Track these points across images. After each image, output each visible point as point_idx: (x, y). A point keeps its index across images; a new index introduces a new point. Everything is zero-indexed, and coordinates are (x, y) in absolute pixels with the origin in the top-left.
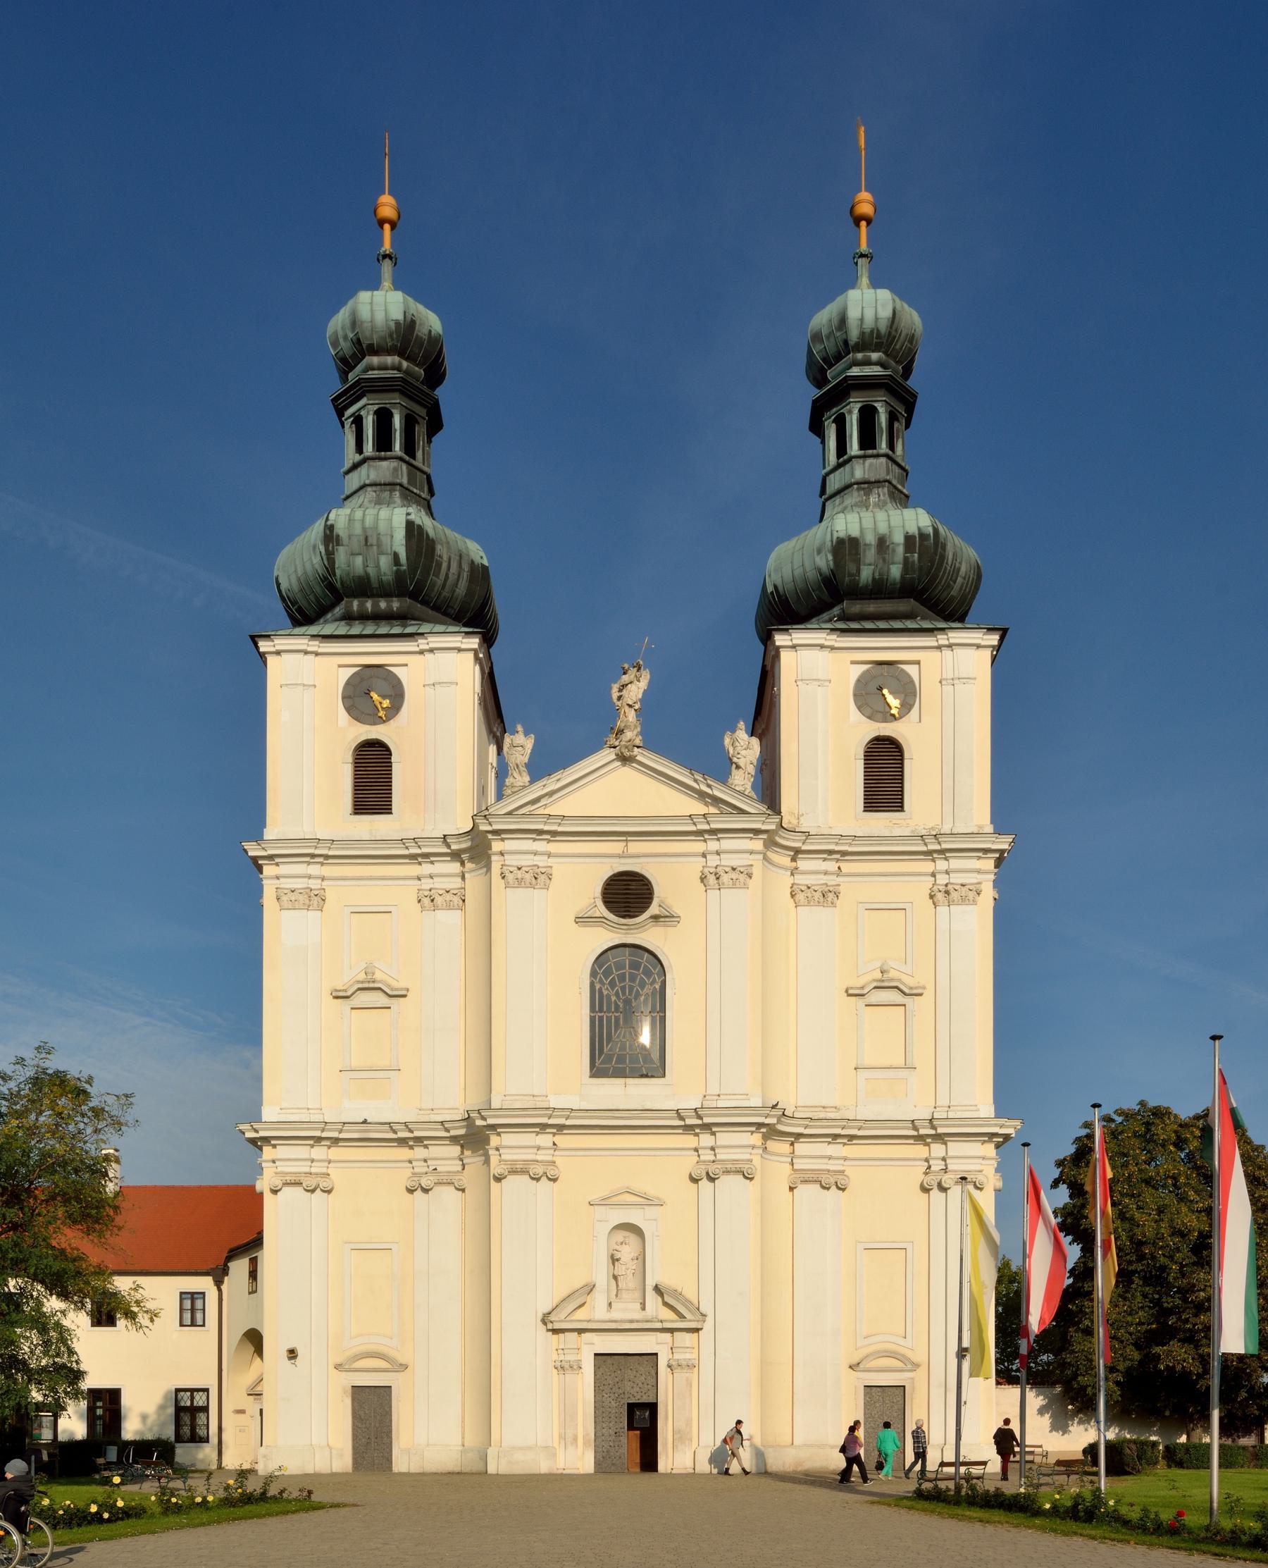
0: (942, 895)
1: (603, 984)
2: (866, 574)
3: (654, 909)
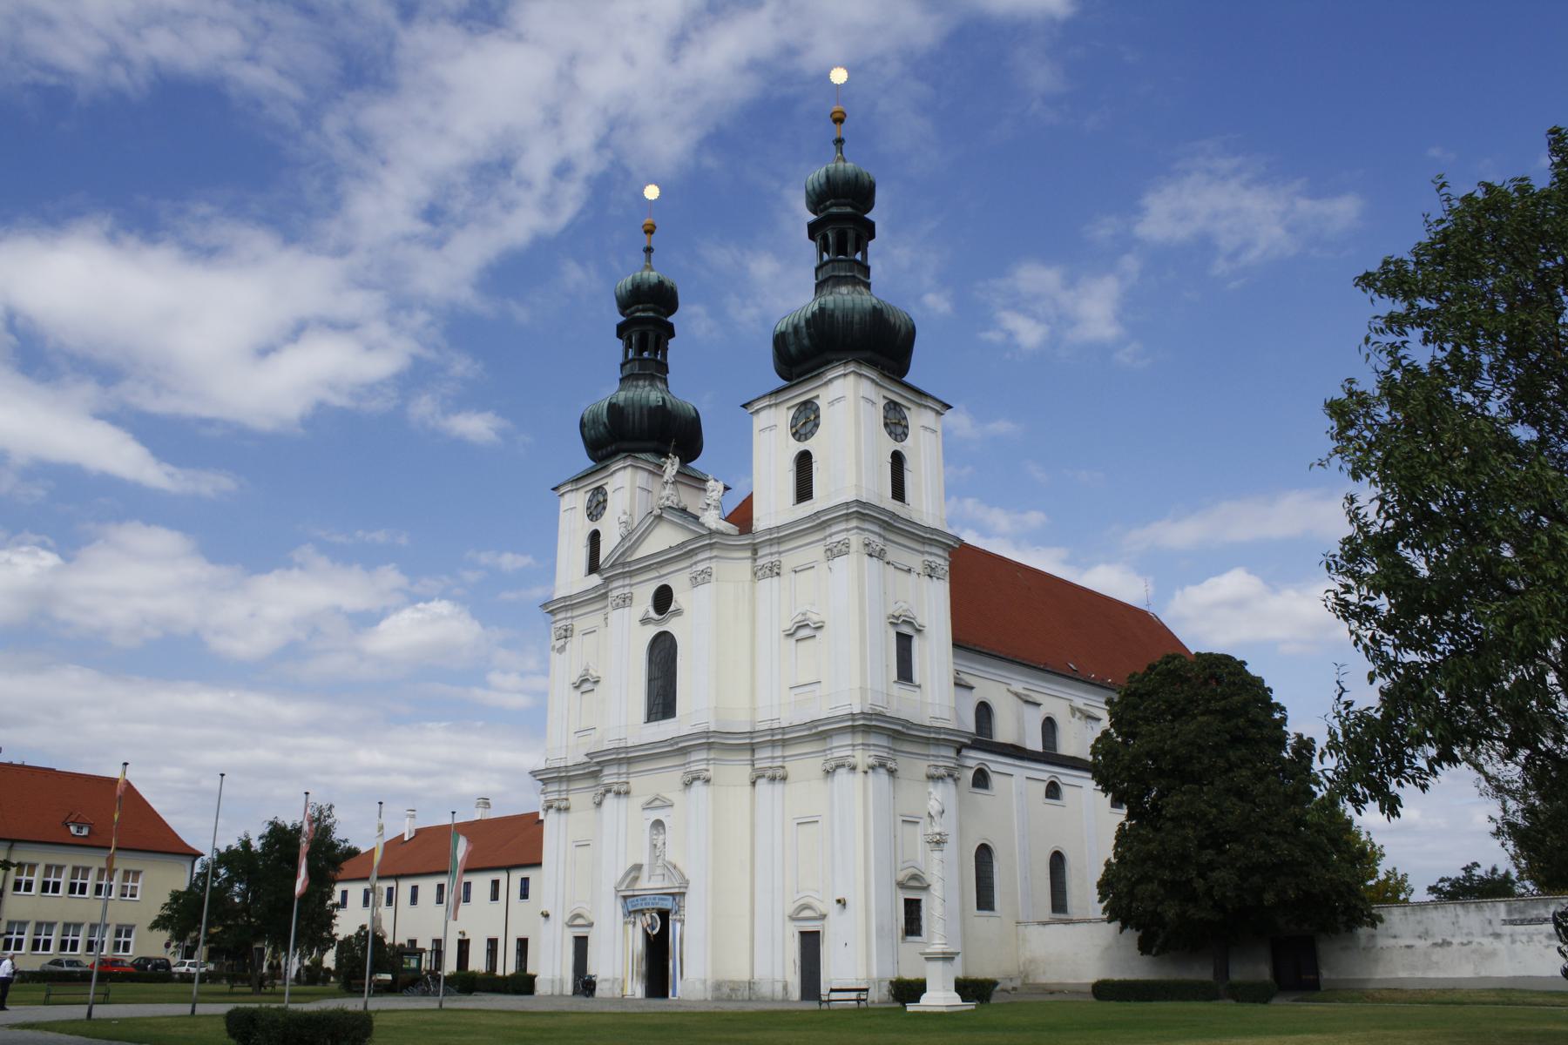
0: (832, 553)
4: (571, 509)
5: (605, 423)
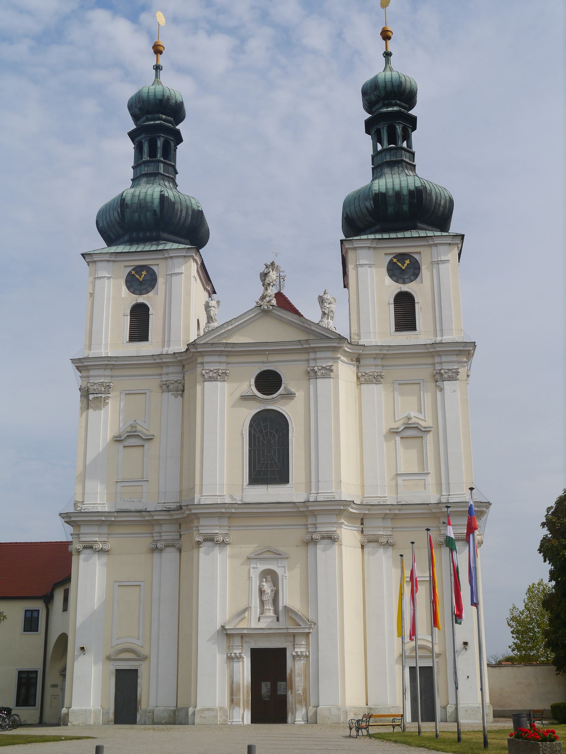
1: (256, 432)
3: (281, 391)
5: (155, 211)
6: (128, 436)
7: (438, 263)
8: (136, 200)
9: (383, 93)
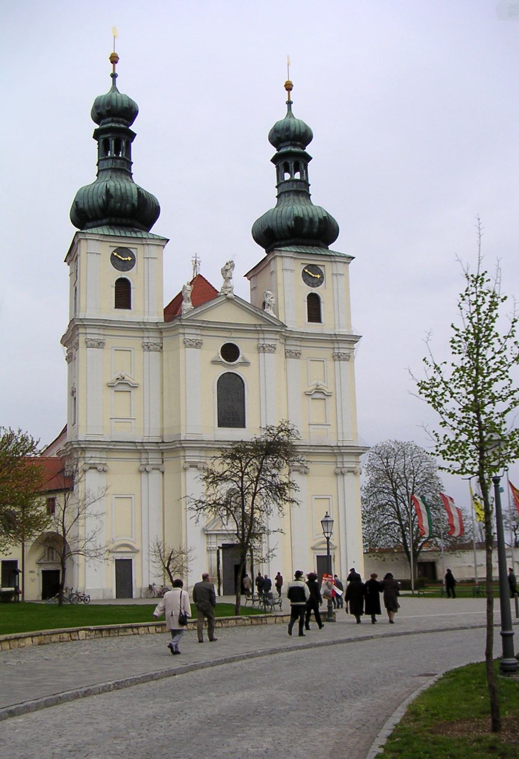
2: (305, 230)
3: (239, 360)
4: (97, 254)
5: (133, 205)
6: (119, 383)
7: (336, 275)
8: (119, 193)
9: (292, 135)
